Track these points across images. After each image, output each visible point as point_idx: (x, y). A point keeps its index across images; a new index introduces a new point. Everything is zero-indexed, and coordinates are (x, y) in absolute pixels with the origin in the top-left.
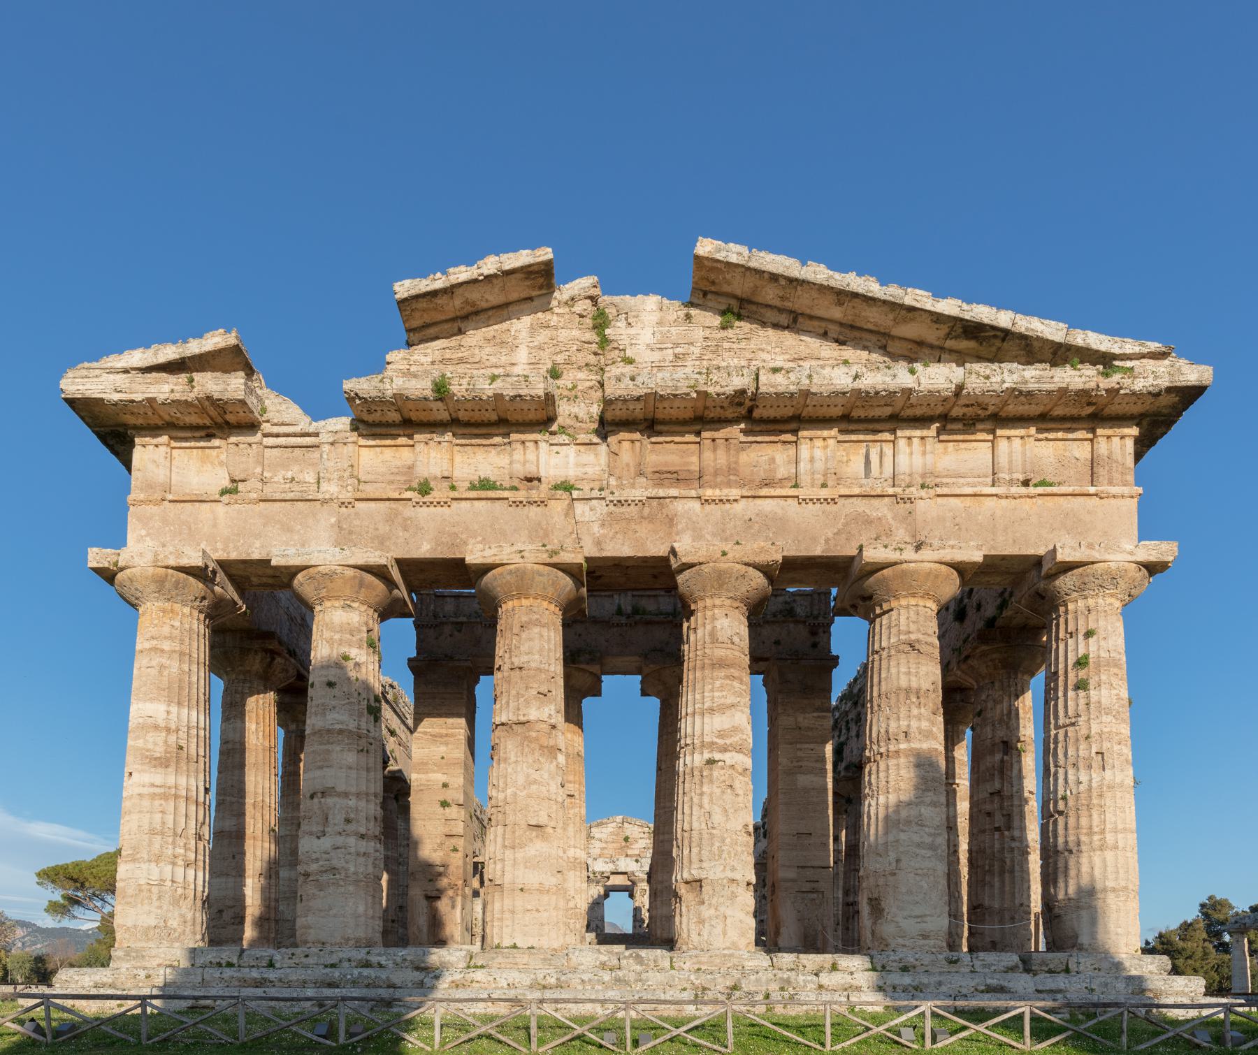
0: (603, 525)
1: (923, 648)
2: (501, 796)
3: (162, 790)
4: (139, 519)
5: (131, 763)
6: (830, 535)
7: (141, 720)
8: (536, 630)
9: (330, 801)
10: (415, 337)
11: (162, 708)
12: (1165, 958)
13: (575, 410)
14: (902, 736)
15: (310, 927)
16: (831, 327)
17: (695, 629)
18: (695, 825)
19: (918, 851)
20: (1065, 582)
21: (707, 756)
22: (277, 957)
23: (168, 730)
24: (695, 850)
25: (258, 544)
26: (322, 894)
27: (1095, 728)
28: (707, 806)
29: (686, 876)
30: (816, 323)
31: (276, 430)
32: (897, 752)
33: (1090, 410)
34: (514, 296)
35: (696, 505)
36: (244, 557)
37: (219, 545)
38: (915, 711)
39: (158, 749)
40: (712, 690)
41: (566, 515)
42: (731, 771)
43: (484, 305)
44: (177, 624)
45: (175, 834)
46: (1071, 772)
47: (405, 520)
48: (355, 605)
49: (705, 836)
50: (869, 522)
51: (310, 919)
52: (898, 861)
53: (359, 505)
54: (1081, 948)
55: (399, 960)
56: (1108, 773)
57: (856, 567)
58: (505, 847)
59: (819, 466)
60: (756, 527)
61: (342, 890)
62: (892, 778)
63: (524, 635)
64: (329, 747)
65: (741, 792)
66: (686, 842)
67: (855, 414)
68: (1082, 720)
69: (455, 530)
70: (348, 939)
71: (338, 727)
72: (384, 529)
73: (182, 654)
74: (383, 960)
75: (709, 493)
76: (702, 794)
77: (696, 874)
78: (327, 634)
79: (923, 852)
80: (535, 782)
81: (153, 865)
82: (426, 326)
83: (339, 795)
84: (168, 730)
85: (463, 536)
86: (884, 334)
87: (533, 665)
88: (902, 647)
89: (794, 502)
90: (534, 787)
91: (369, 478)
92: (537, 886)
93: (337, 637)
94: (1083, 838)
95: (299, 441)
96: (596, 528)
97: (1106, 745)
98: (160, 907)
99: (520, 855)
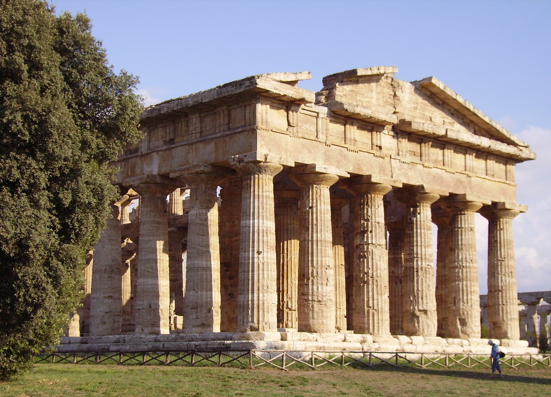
2: (375, 274)
17: (419, 214)
18: (424, 289)
21: (427, 263)
22: (318, 337)
24: (424, 298)
26: (328, 311)
27: (510, 264)
28: (428, 282)
29: (421, 308)
32: (469, 267)
35: (422, 166)
40: (428, 238)
46: (503, 277)
49: (428, 294)
50: (461, 182)
52: (471, 306)
53: (332, 146)
54: (508, 338)
56: (513, 279)
58: (378, 293)
62: (468, 276)
63: (379, 209)
66: (420, 295)
68: (506, 259)
69: (359, 163)
75: (426, 164)
76: (426, 278)
77: (425, 308)
89: (444, 171)
94: (508, 301)
96: (397, 171)
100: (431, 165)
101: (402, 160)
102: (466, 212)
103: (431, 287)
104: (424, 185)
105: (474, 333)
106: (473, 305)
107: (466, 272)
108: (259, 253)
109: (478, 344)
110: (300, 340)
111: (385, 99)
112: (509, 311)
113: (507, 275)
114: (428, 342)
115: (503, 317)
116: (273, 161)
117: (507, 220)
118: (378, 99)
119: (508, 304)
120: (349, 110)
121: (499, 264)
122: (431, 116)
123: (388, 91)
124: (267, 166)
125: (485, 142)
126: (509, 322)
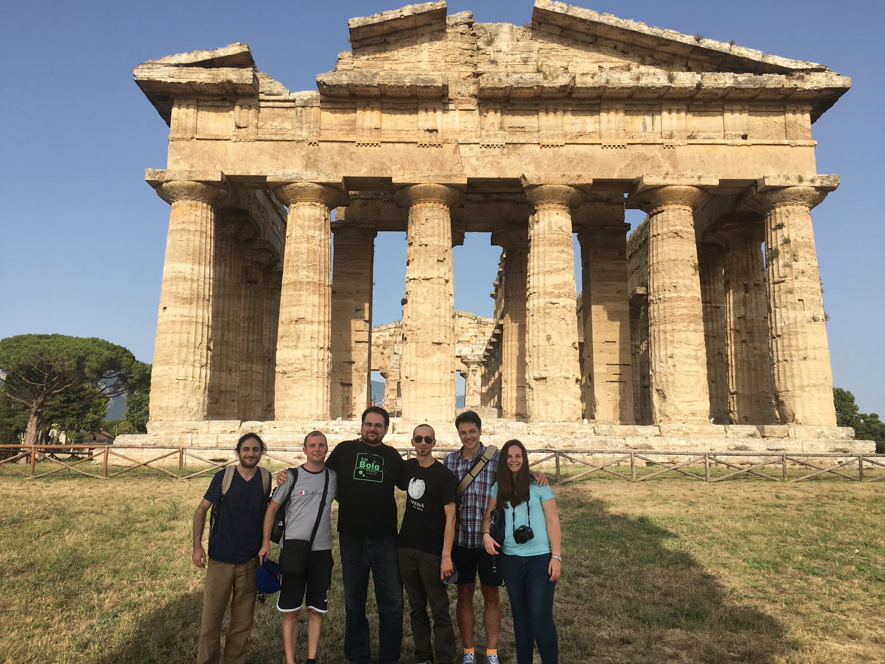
0: (478, 159)
1: (685, 235)
3: (187, 319)
4: (176, 150)
5: (165, 301)
6: (622, 166)
7: (174, 274)
8: (436, 221)
9: (301, 326)
10: (357, 45)
11: (190, 266)
12: (851, 429)
13: (459, 89)
14: (672, 289)
15: (287, 408)
16: (619, 44)
18: (541, 343)
19: (686, 360)
20: (774, 197)
21: (548, 300)
23: (192, 280)
25: (254, 166)
26: (295, 386)
30: (610, 42)
31: (267, 98)
33: (781, 96)
34: (422, 23)
35: (538, 147)
36: (245, 174)
37: (229, 166)
38: (681, 274)
39: (186, 293)
40: (550, 260)
41: (455, 152)
42: (564, 310)
43: (402, 28)
44: (199, 214)
45: (195, 347)
47: (351, 154)
48: (318, 204)
50: (646, 159)
51: (288, 402)
53: (321, 144)
55: (348, 428)
57: (640, 187)
59: (613, 125)
60: (575, 161)
61: (309, 383)
62: (667, 314)
63: (429, 225)
64: (302, 293)
65: (570, 323)
66: (535, 353)
67: (635, 96)
69: (383, 160)
70: (312, 415)
71: (308, 280)
72: (337, 159)
73: (201, 232)
74: (337, 429)
75: (545, 142)
76: (545, 323)
77: (544, 375)
78: (300, 222)
79: (689, 361)
80: (436, 315)
81: (181, 367)
82: (364, 39)
83: (307, 323)
84: (192, 280)
85: (389, 164)
86: (652, 49)
87: (436, 243)
88: (670, 234)
90: (437, 318)
91: (327, 127)
92: (438, 381)
93: (306, 224)
94: (793, 352)
95: (282, 104)
96: (473, 161)
97: (804, 296)
98: (184, 394)
99: (428, 361)
100: (561, 141)
101: (486, 142)
102: (665, 208)
103: (554, 339)
104: (526, 174)
105: (679, 412)
106: (677, 364)
107: (665, 309)
108: (165, 308)
109: (686, 434)
110: (224, 432)
111: (448, 59)
112: (795, 372)
113: (789, 306)
114: (538, 432)
115: (786, 383)
116: (177, 177)
117: (789, 208)
118: (432, 62)
119: (794, 359)
120: (327, 83)
121: (777, 289)
122: (565, 64)
123: (458, 44)
124: (172, 188)
125: (686, 79)
126: (798, 392)
